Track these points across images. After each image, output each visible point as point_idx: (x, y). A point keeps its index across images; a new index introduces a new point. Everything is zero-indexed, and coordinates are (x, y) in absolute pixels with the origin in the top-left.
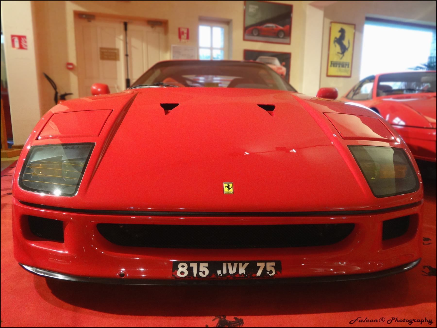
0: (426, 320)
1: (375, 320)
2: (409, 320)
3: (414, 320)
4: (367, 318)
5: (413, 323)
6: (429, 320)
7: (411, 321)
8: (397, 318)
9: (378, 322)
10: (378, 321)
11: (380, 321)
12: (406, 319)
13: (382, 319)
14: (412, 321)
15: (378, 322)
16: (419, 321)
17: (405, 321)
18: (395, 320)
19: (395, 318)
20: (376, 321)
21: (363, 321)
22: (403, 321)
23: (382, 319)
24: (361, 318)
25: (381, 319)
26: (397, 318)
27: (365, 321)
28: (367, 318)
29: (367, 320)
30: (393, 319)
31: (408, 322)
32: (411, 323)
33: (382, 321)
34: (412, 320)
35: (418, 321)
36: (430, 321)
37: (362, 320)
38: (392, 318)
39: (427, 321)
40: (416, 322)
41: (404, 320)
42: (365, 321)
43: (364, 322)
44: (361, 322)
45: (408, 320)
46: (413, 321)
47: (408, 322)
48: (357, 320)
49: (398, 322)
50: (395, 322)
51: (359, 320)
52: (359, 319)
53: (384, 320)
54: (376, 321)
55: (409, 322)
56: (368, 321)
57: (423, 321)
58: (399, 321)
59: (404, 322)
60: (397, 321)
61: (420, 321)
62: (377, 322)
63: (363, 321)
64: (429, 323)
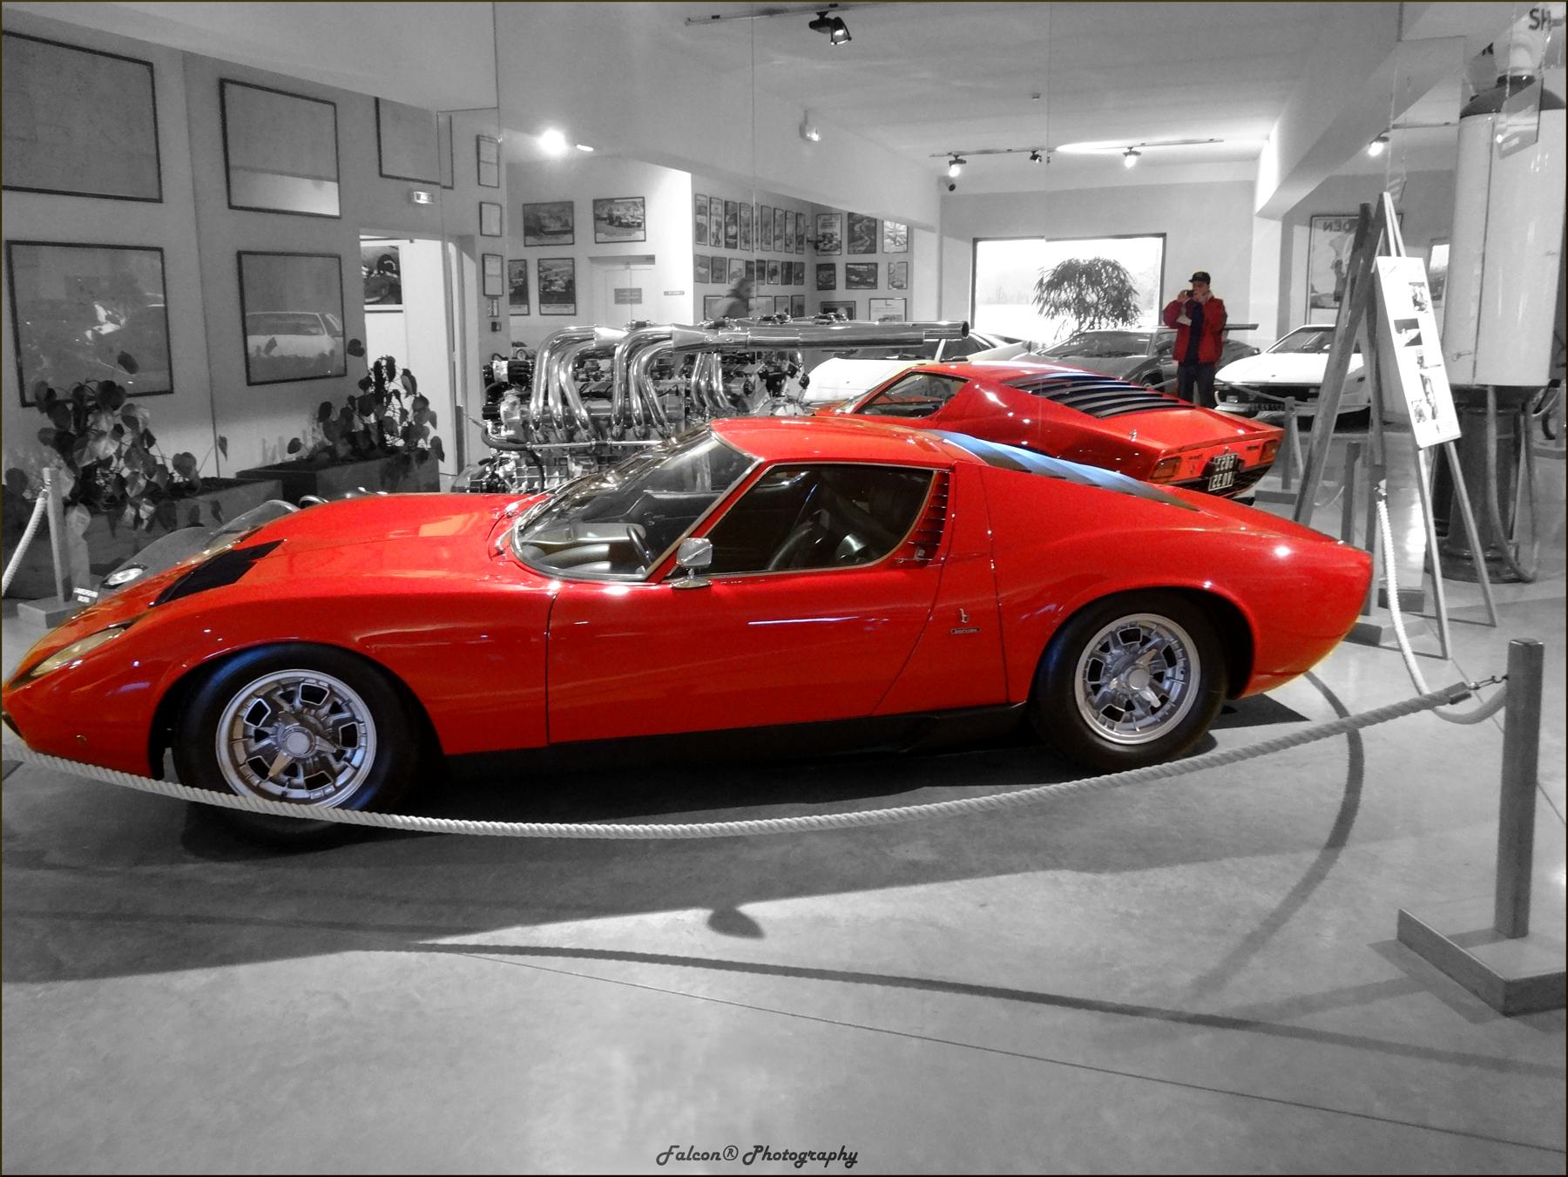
0: (842, 1153)
1: (714, 1154)
2: (798, 1154)
3: (811, 1154)
4: (692, 1147)
5: (806, 1162)
6: (851, 1154)
7: (802, 1156)
8: (768, 1147)
9: (720, 1159)
10: (721, 1156)
11: (726, 1155)
12: (790, 1152)
13: (731, 1151)
14: (805, 1157)
15: (720, 1159)
16: (823, 1158)
17: (787, 1156)
18: (763, 1153)
19: (762, 1147)
20: (716, 1156)
21: (685, 1156)
22: (782, 1156)
23: (731, 1151)
24: (678, 1147)
25: (727, 1151)
26: (768, 1147)
27: (691, 1157)
28: (692, 1147)
29: (694, 1157)
30: (758, 1148)
31: (794, 1161)
32: (803, 1161)
33: (730, 1157)
34: (805, 1154)
35: (821, 1156)
36: (852, 1156)
37: (683, 1154)
38: (755, 1147)
39: (844, 1159)
40: (815, 1159)
41: (786, 1152)
42: (691, 1157)
43: (689, 1159)
44: (682, 1159)
45: (796, 1154)
46: (808, 1158)
47: (794, 1161)
48: (670, 1153)
49: (769, 1159)
50: (763, 1159)
51: (675, 1155)
52: (674, 1150)
53: (734, 1153)
54: (716, 1156)
55: (797, 1159)
56: (696, 1156)
57: (833, 1156)
58: (772, 1157)
59: (785, 1159)
60: (767, 1156)
61: (827, 1156)
62: (718, 1159)
63: (685, 1156)
64: (846, 1164)
